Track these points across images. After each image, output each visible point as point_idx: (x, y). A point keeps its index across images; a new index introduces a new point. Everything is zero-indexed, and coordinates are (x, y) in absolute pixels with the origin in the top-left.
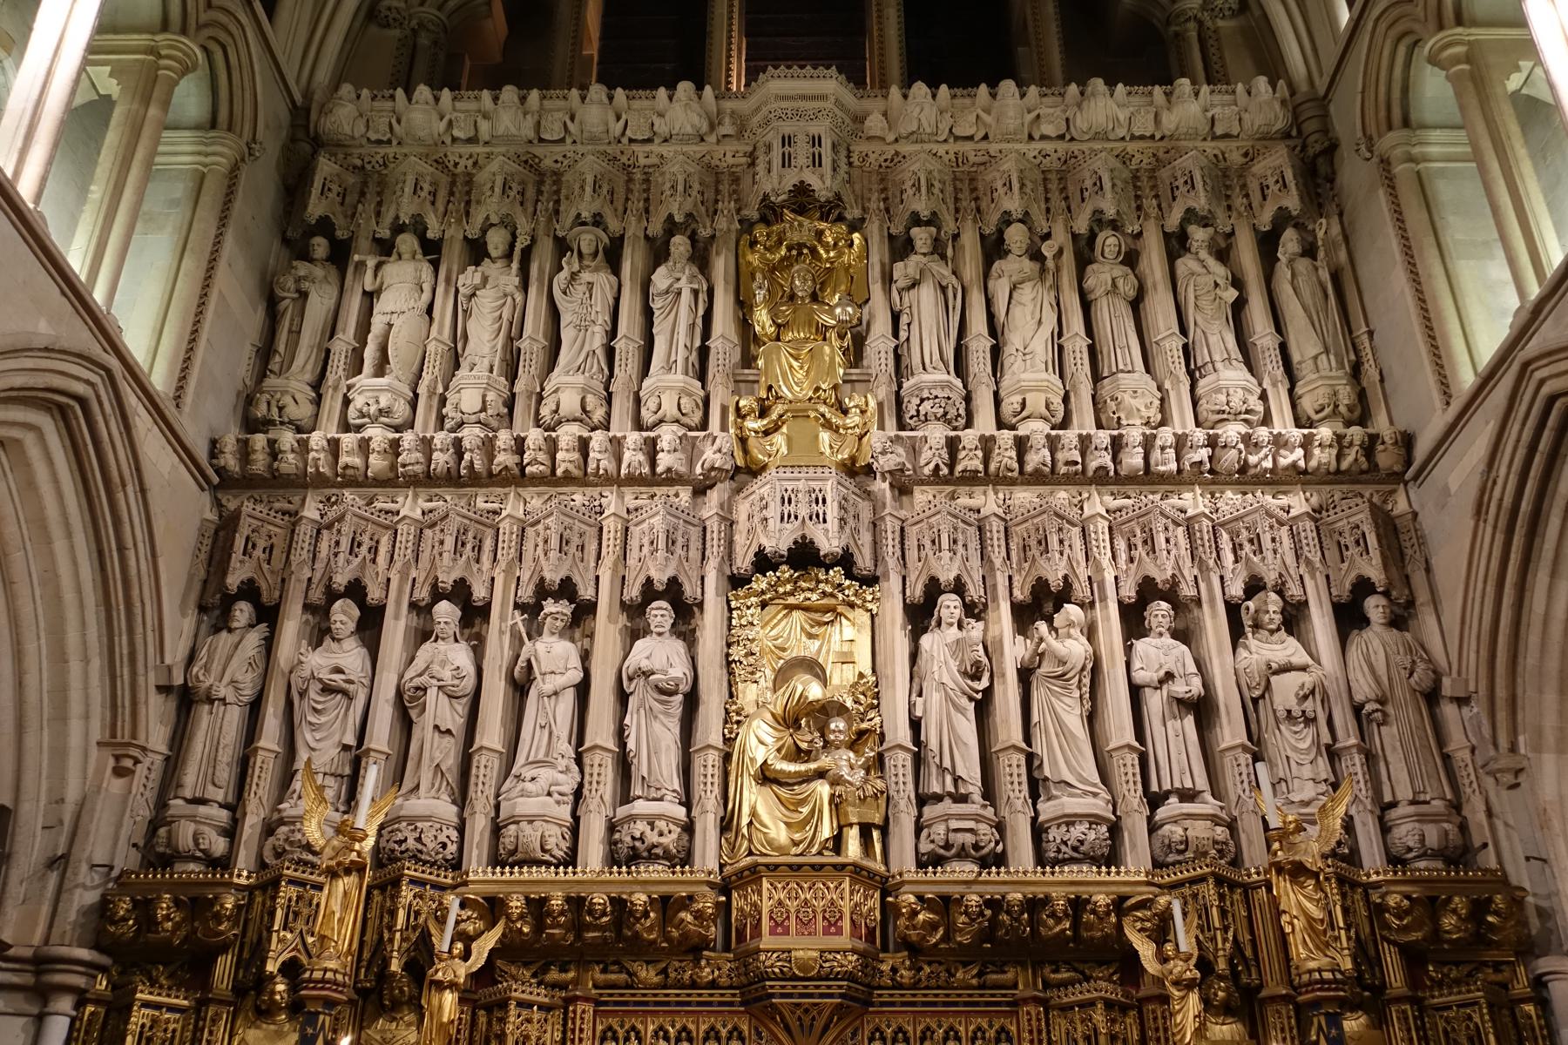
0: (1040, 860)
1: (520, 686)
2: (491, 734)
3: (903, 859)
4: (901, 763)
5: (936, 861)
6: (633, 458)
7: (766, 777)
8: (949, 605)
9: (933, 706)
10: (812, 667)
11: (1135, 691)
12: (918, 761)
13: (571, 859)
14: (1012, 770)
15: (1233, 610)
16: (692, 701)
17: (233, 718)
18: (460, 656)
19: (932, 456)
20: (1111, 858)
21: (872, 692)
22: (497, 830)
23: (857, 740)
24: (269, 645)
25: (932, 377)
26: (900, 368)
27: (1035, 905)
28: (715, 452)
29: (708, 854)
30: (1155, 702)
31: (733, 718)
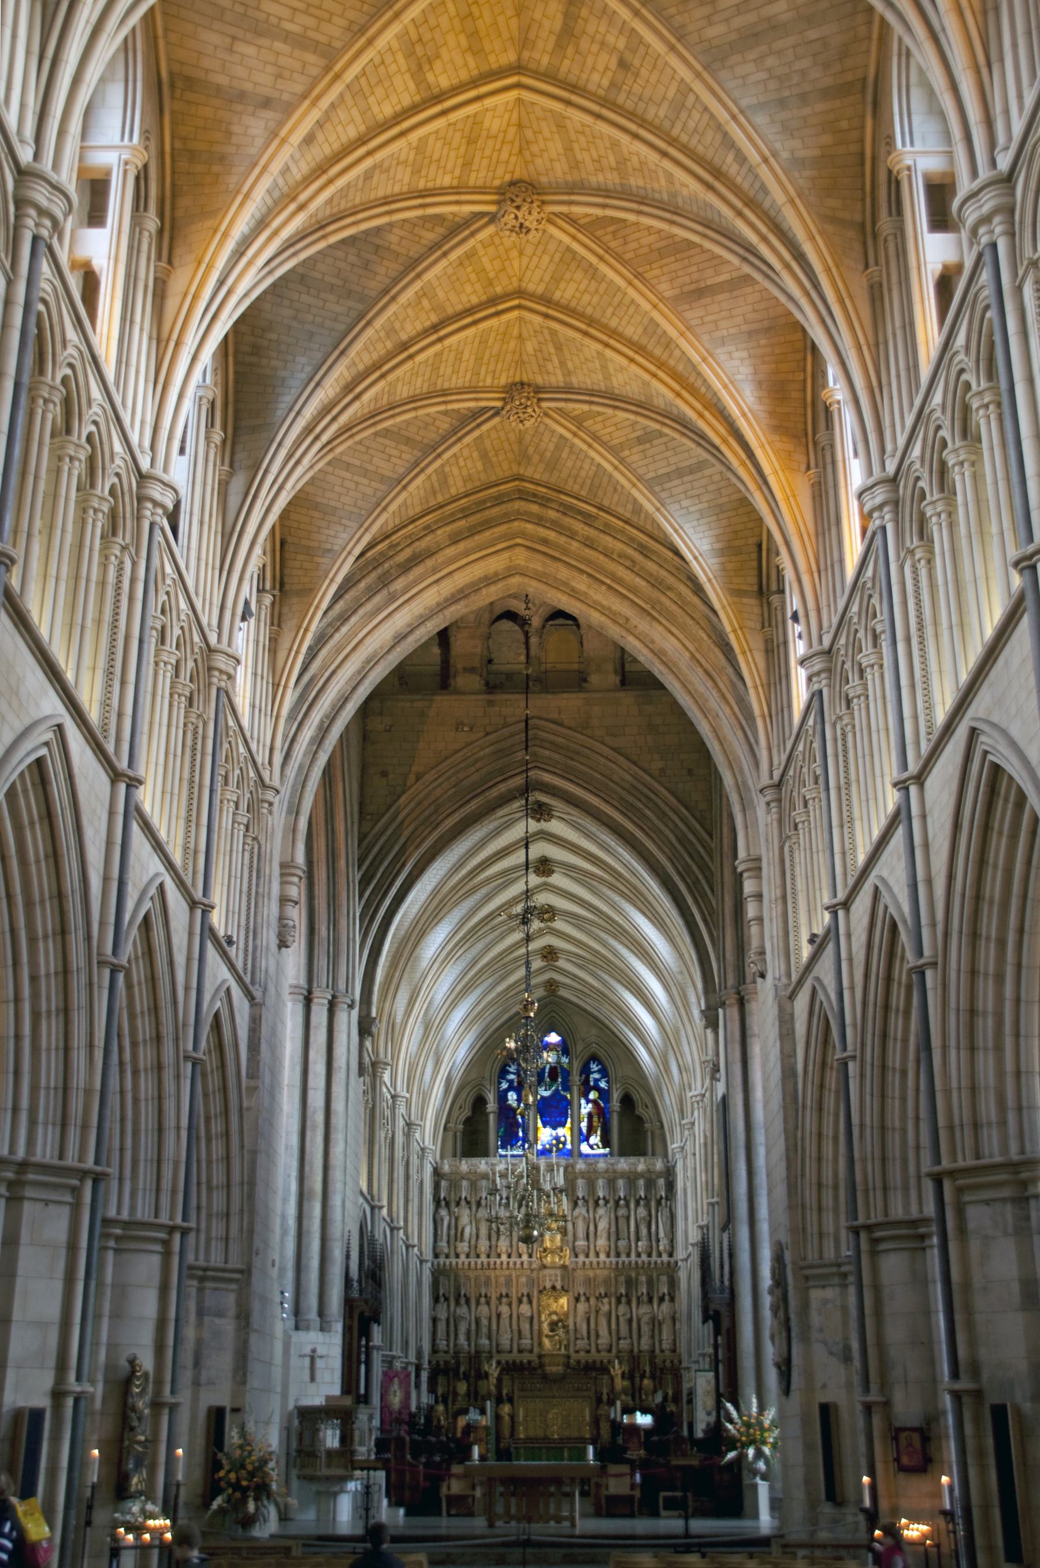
0: (598, 1351)
1: (499, 1316)
2: (494, 1327)
4: (572, 1333)
6: (518, 1266)
7: (547, 1336)
8: (582, 1299)
9: (579, 1320)
10: (555, 1313)
11: (617, 1317)
12: (576, 1330)
13: (510, 1352)
14: (593, 1333)
15: (638, 1299)
16: (532, 1318)
20: (610, 1351)
21: (567, 1315)
22: (497, 1345)
24: (448, 1306)
25: (581, 1243)
27: (594, 1362)
29: (536, 1350)
30: (621, 1319)
31: (540, 1322)
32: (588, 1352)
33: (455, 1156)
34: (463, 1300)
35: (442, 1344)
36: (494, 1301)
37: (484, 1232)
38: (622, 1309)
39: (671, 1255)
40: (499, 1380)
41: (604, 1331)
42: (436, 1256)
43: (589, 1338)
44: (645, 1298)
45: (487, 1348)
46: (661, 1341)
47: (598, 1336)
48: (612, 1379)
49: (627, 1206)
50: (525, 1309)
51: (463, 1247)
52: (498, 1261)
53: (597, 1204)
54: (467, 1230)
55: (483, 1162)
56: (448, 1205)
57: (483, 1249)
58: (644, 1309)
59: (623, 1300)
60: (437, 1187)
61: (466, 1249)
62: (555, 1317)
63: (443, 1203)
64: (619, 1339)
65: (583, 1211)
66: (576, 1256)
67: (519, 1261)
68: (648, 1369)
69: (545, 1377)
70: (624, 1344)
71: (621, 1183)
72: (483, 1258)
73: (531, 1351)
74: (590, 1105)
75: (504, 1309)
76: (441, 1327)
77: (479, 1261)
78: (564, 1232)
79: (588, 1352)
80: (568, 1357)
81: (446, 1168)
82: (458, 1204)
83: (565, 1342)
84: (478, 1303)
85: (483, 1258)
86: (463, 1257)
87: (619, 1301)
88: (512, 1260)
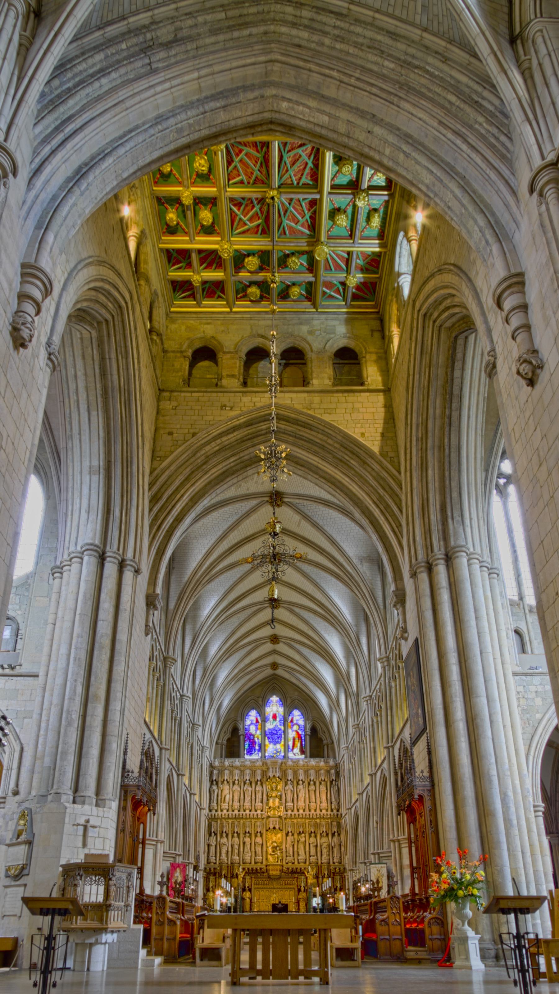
0: (299, 863)
1: (244, 843)
3: (284, 863)
4: (284, 853)
5: (287, 863)
6: (255, 816)
8: (290, 834)
9: (288, 846)
10: (275, 842)
16: (262, 845)
17: (214, 847)
18: (237, 839)
19: (289, 816)
20: (305, 863)
21: (281, 843)
23: (280, 849)
25: (290, 804)
26: (286, 801)
27: (297, 869)
28: (265, 815)
29: (264, 863)
30: (311, 845)
31: (267, 847)
32: (293, 863)
33: (221, 757)
34: (224, 835)
35: (213, 859)
36: (242, 835)
37: (236, 798)
38: (312, 840)
39: (338, 811)
40: (244, 878)
41: (302, 852)
42: (210, 811)
43: (293, 856)
44: (325, 834)
45: (237, 861)
46: (333, 857)
47: (298, 855)
48: (307, 878)
49: (315, 784)
50: (259, 840)
51: (225, 806)
52: (244, 813)
53: (298, 784)
54: (227, 797)
55: (237, 760)
56: (217, 783)
57: (236, 807)
58: (324, 840)
59: (313, 835)
60: (211, 774)
61: (227, 807)
62: (275, 845)
63: (215, 782)
64: (310, 856)
65: (291, 787)
66: (287, 811)
67: (255, 813)
68: (326, 873)
69: (269, 877)
70: (313, 859)
71: (312, 772)
72: (236, 812)
73: (262, 863)
74: (294, 733)
75: (247, 840)
76: (212, 849)
77: (234, 813)
78: (280, 799)
79: (293, 863)
80: (282, 866)
81: (217, 764)
82: (222, 783)
83: (280, 858)
84: (233, 837)
85: (236, 812)
86: (225, 811)
87: (310, 836)
88: (251, 813)
